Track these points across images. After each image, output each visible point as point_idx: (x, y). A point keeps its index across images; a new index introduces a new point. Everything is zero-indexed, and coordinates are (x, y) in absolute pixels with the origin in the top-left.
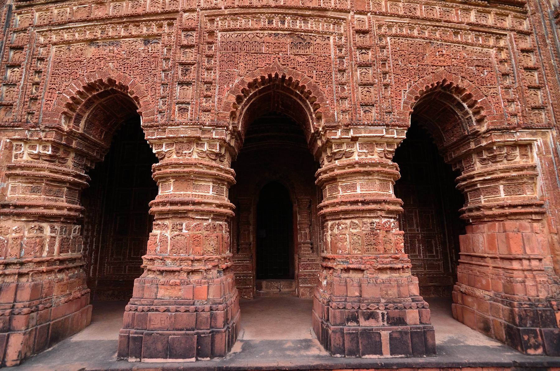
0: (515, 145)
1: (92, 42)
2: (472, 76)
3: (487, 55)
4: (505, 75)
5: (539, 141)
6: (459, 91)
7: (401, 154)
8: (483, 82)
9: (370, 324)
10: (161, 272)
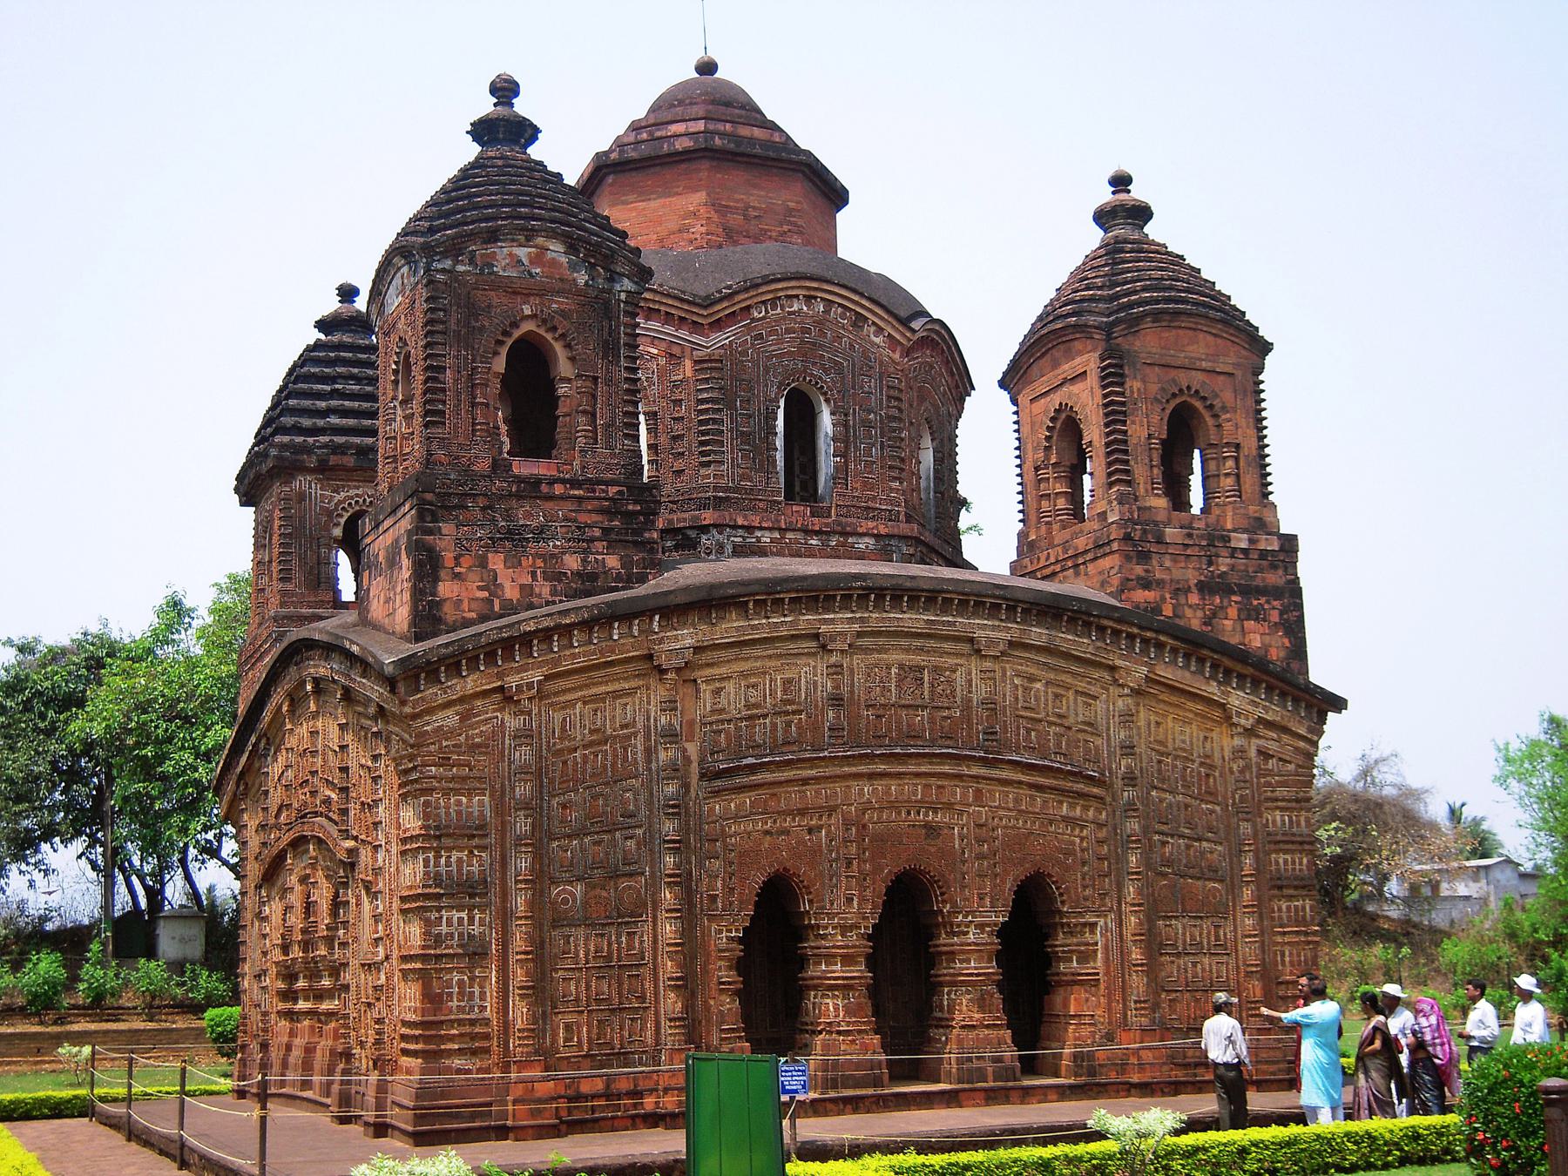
0: (1084, 925)
1: (767, 832)
2: (1059, 862)
3: (1073, 843)
4: (1084, 863)
5: (1101, 922)
6: (1050, 876)
7: (1003, 932)
8: (1067, 869)
9: (981, 1064)
10: (839, 1033)
